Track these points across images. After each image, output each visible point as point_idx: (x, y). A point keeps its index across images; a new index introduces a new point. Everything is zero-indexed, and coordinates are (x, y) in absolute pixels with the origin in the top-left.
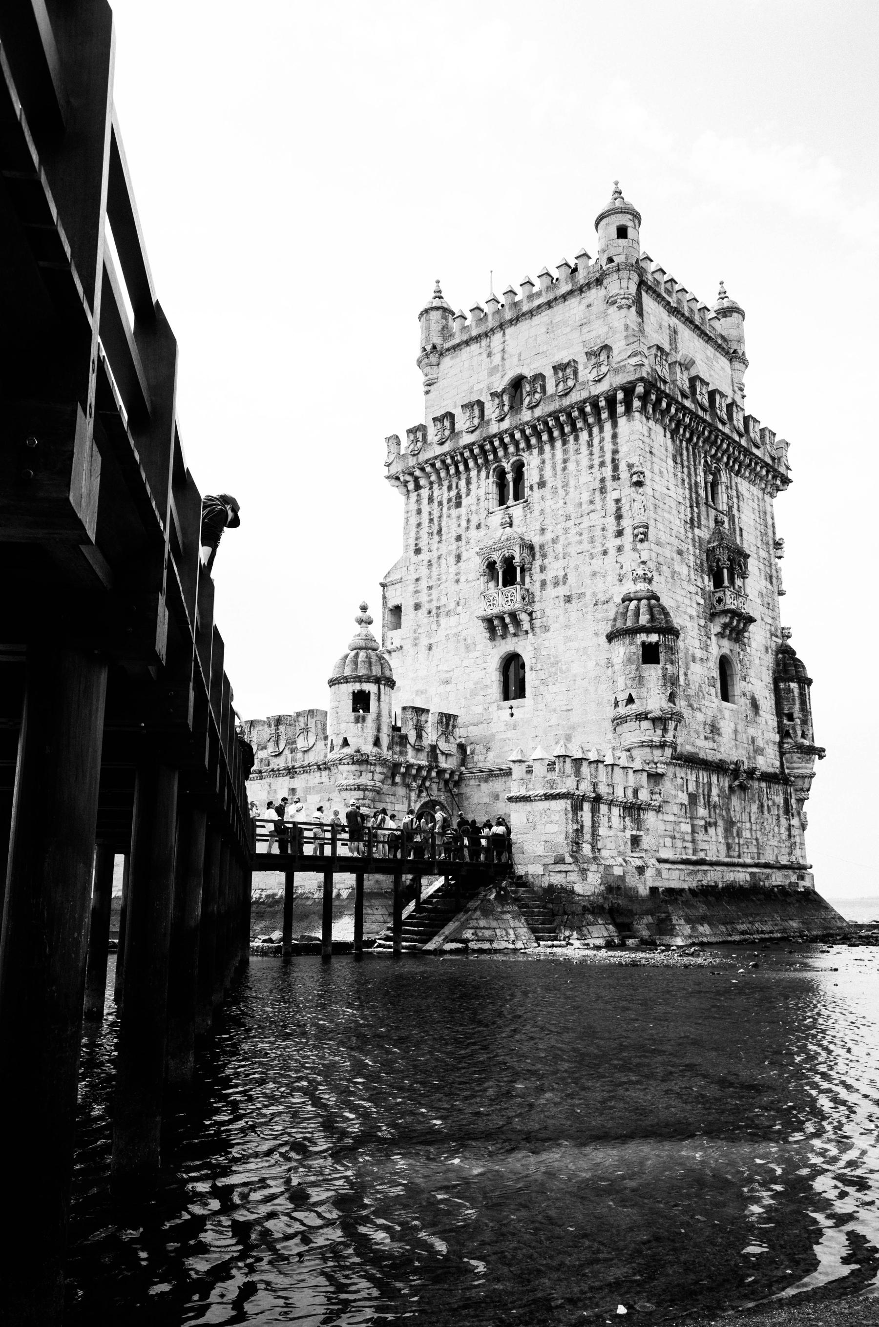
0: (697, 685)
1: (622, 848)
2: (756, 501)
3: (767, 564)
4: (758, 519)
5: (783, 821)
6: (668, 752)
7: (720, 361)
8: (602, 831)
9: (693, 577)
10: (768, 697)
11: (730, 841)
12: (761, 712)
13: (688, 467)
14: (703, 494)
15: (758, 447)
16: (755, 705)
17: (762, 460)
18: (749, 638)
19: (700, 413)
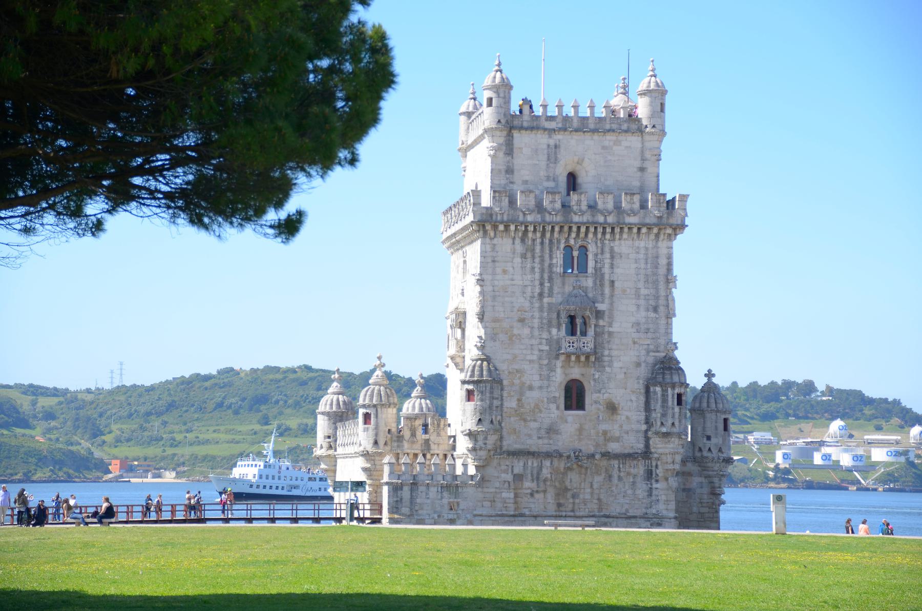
0: (532, 405)
1: (439, 509)
2: (643, 251)
4: (643, 266)
6: (483, 453)
7: (624, 144)
8: (418, 501)
9: (536, 333)
10: (634, 398)
11: (561, 501)
13: (542, 257)
14: (559, 270)
16: (612, 408)
17: (635, 224)
18: (611, 361)
19: (548, 218)
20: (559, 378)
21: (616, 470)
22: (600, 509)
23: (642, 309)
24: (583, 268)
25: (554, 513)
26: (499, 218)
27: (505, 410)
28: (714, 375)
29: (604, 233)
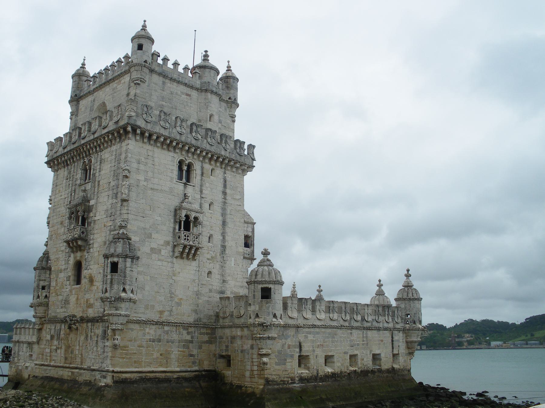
2: (114, 153)
3: (115, 187)
5: (100, 344)
7: (122, 81)
10: (101, 271)
12: (94, 283)
13: (73, 175)
15: (106, 127)
16: (91, 280)
17: (104, 134)
18: (93, 244)
20: (72, 261)
21: (90, 332)
22: (82, 363)
23: (110, 198)
24: (90, 179)
25: (61, 365)
26: (55, 156)
27: (52, 288)
28: (269, 254)
29: (96, 148)
